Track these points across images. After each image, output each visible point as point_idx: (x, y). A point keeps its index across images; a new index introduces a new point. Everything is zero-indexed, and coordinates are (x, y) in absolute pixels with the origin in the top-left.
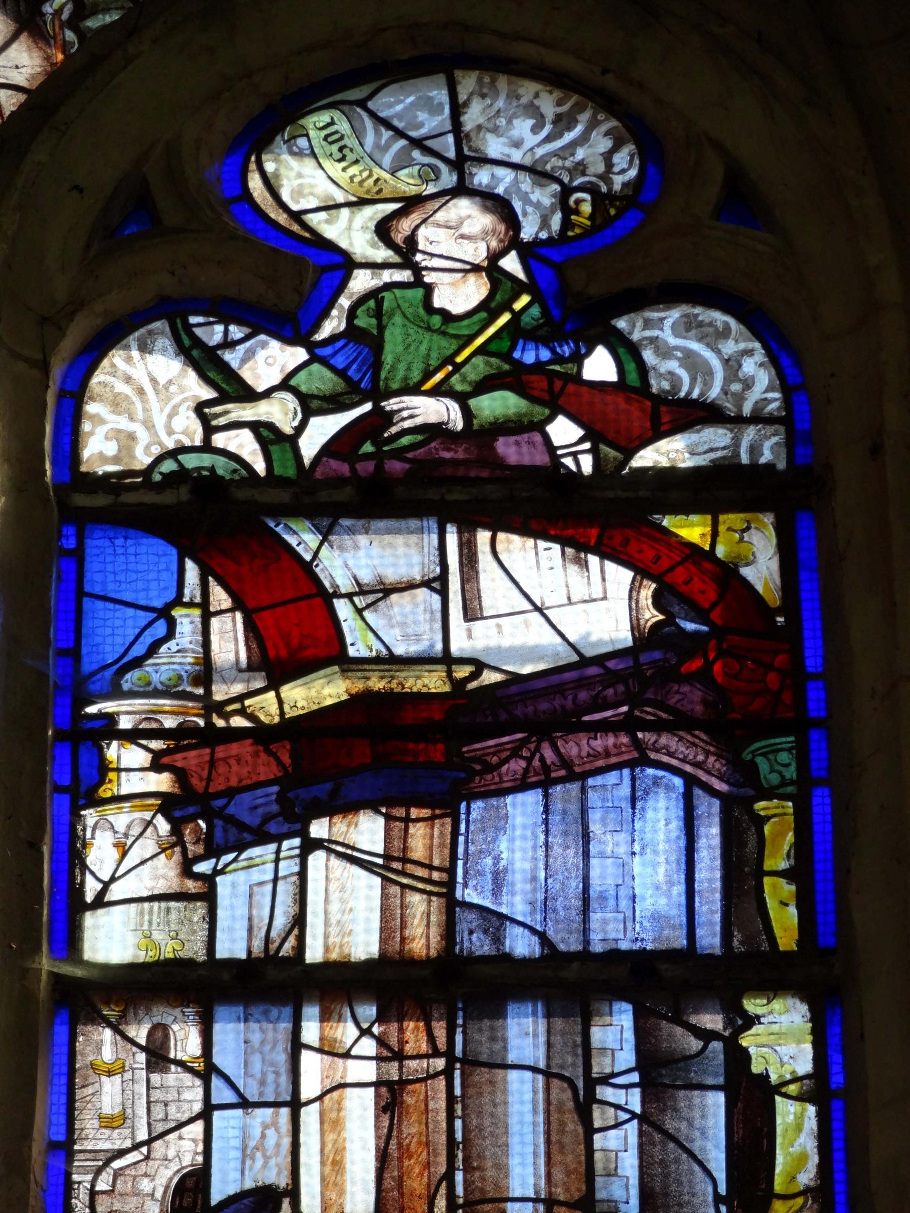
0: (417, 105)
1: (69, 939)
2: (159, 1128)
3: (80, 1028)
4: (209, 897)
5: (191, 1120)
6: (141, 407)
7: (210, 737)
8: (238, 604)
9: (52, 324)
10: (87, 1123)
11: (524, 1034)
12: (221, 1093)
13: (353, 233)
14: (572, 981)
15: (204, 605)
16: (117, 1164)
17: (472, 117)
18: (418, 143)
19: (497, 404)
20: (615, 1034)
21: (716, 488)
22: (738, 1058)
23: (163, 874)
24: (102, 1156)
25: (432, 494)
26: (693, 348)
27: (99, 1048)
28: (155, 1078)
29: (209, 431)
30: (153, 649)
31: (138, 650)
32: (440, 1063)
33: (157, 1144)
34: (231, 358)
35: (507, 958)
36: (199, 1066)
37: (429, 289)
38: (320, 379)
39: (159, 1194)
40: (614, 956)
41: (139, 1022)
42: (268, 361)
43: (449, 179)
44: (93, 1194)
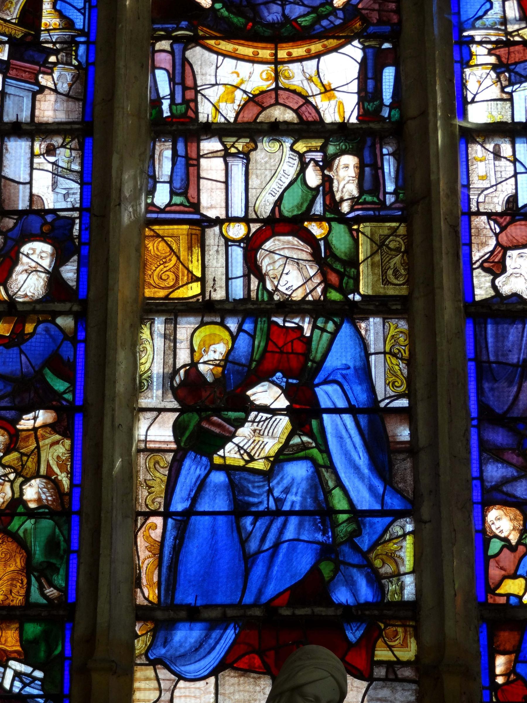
1: (463, 114)
2: (500, 180)
3: (469, 145)
4: (511, 100)
5: (510, 178)
7: (508, 44)
12: (520, 168)
16: (486, 192)
23: (495, 92)
24: (480, 190)
27: (476, 153)
28: (497, 163)
30: (486, 13)
31: (480, 13)
33: (499, 186)
36: (512, 159)
39: (501, 203)
41: (490, 143)
44: (478, 203)
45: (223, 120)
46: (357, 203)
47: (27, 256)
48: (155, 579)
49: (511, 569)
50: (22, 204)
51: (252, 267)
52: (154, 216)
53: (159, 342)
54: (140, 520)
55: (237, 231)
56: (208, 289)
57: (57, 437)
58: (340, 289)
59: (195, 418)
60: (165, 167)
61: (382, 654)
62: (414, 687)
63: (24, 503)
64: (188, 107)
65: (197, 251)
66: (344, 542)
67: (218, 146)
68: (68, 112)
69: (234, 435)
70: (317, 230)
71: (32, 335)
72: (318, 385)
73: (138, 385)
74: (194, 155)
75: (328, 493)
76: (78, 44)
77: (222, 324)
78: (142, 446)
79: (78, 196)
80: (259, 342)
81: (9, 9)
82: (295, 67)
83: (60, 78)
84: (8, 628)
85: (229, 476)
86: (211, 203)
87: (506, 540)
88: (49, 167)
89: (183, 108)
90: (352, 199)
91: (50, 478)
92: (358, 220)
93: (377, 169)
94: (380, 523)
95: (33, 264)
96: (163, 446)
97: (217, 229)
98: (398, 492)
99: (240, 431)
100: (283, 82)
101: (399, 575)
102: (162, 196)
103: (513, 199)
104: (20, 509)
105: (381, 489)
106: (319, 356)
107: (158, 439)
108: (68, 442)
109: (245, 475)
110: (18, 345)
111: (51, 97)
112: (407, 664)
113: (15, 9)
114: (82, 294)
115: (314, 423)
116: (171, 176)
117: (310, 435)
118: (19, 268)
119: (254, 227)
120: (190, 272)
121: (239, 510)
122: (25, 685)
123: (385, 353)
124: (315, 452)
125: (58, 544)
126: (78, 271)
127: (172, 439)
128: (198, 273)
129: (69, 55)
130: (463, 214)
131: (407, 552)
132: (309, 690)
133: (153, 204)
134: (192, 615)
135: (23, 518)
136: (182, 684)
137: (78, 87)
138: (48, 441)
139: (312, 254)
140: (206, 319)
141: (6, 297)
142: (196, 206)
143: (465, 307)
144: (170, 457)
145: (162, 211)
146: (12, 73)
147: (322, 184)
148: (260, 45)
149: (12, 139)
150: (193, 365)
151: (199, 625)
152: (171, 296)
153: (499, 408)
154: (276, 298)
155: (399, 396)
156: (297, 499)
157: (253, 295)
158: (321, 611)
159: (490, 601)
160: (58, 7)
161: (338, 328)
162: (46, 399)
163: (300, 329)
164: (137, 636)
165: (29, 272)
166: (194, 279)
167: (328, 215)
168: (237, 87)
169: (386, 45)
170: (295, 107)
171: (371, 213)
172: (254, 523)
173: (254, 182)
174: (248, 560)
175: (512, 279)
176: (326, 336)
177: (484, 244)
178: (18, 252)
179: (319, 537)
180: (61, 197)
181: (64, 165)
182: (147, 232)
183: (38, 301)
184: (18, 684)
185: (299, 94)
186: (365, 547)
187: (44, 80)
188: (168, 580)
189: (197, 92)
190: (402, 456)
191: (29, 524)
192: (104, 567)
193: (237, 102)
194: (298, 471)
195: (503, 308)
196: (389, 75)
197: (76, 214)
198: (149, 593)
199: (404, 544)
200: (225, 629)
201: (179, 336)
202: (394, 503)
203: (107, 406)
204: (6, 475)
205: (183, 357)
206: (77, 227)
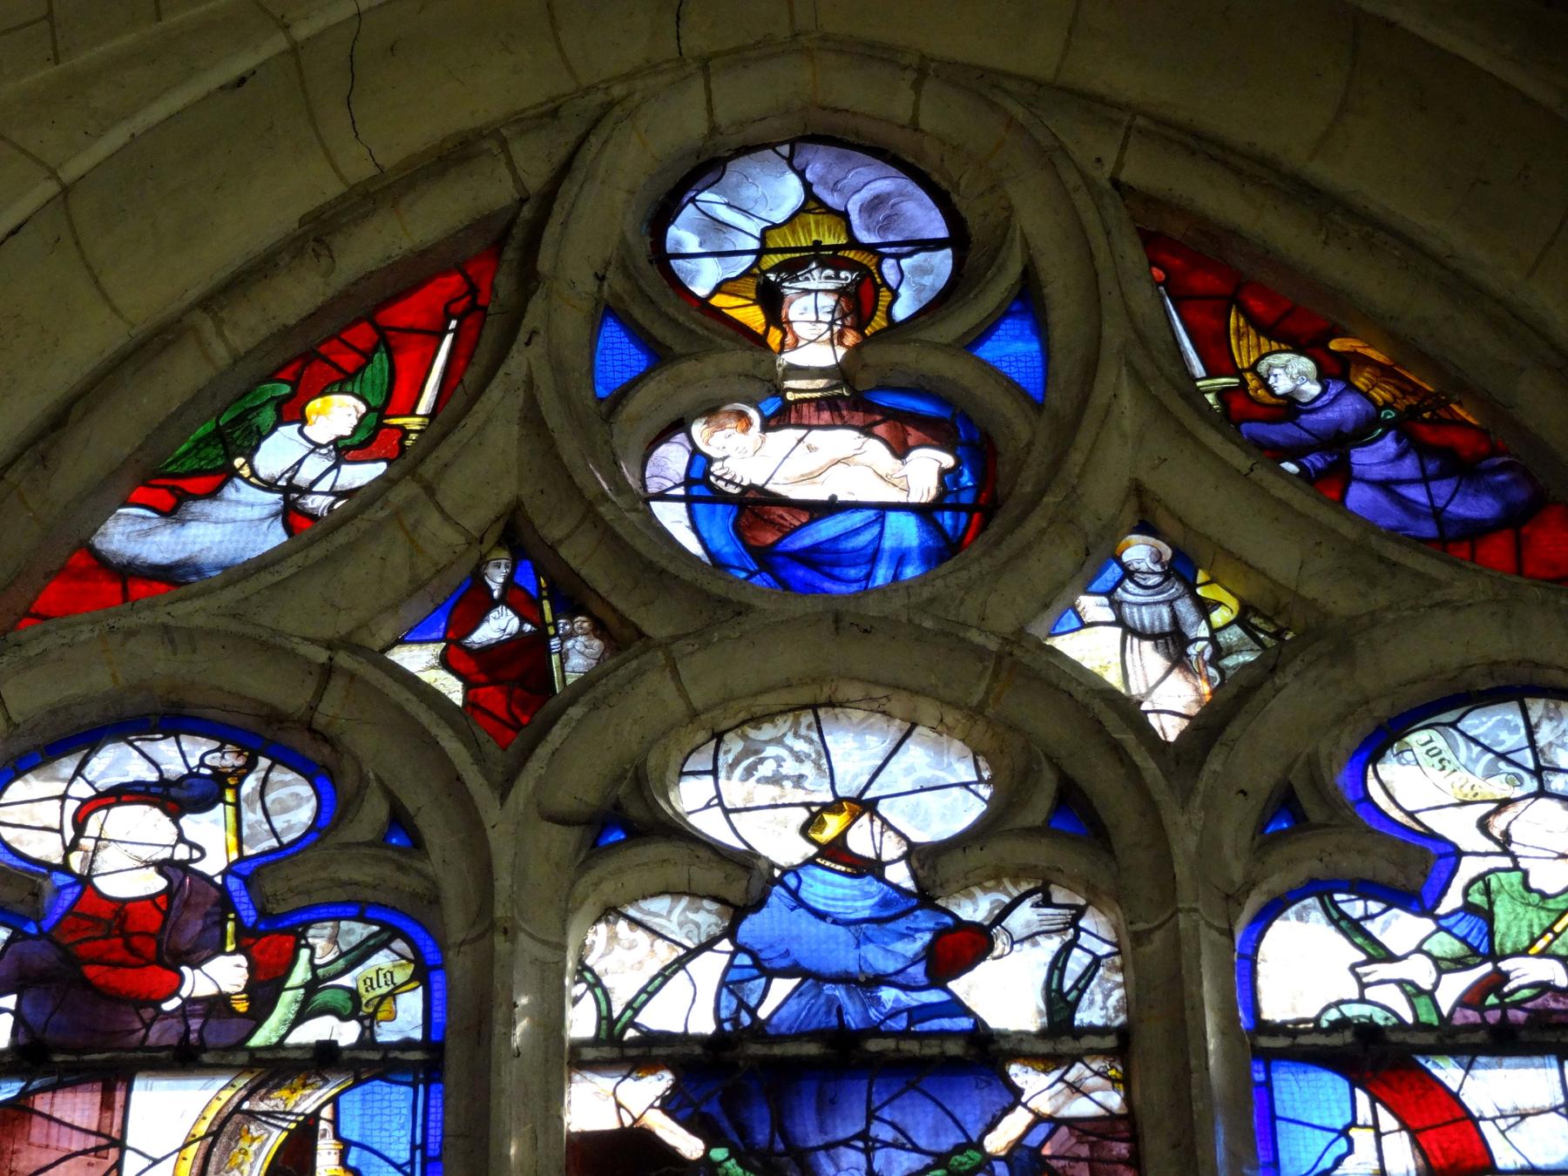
0: (1497, 725)
6: (1302, 968)
8: (1404, 1126)
9: (1233, 899)
13: (1458, 828)
15: (1376, 1126)
17: (1544, 735)
18: (1502, 756)
25: (1550, 1037)
29: (1363, 986)
30: (1338, 1161)
34: (1372, 927)
37: (1526, 874)
38: (1445, 945)
42: (1400, 929)
43: (1531, 785)
81: (239, 1166)
113: (252, 1166)
160: (352, 1162)
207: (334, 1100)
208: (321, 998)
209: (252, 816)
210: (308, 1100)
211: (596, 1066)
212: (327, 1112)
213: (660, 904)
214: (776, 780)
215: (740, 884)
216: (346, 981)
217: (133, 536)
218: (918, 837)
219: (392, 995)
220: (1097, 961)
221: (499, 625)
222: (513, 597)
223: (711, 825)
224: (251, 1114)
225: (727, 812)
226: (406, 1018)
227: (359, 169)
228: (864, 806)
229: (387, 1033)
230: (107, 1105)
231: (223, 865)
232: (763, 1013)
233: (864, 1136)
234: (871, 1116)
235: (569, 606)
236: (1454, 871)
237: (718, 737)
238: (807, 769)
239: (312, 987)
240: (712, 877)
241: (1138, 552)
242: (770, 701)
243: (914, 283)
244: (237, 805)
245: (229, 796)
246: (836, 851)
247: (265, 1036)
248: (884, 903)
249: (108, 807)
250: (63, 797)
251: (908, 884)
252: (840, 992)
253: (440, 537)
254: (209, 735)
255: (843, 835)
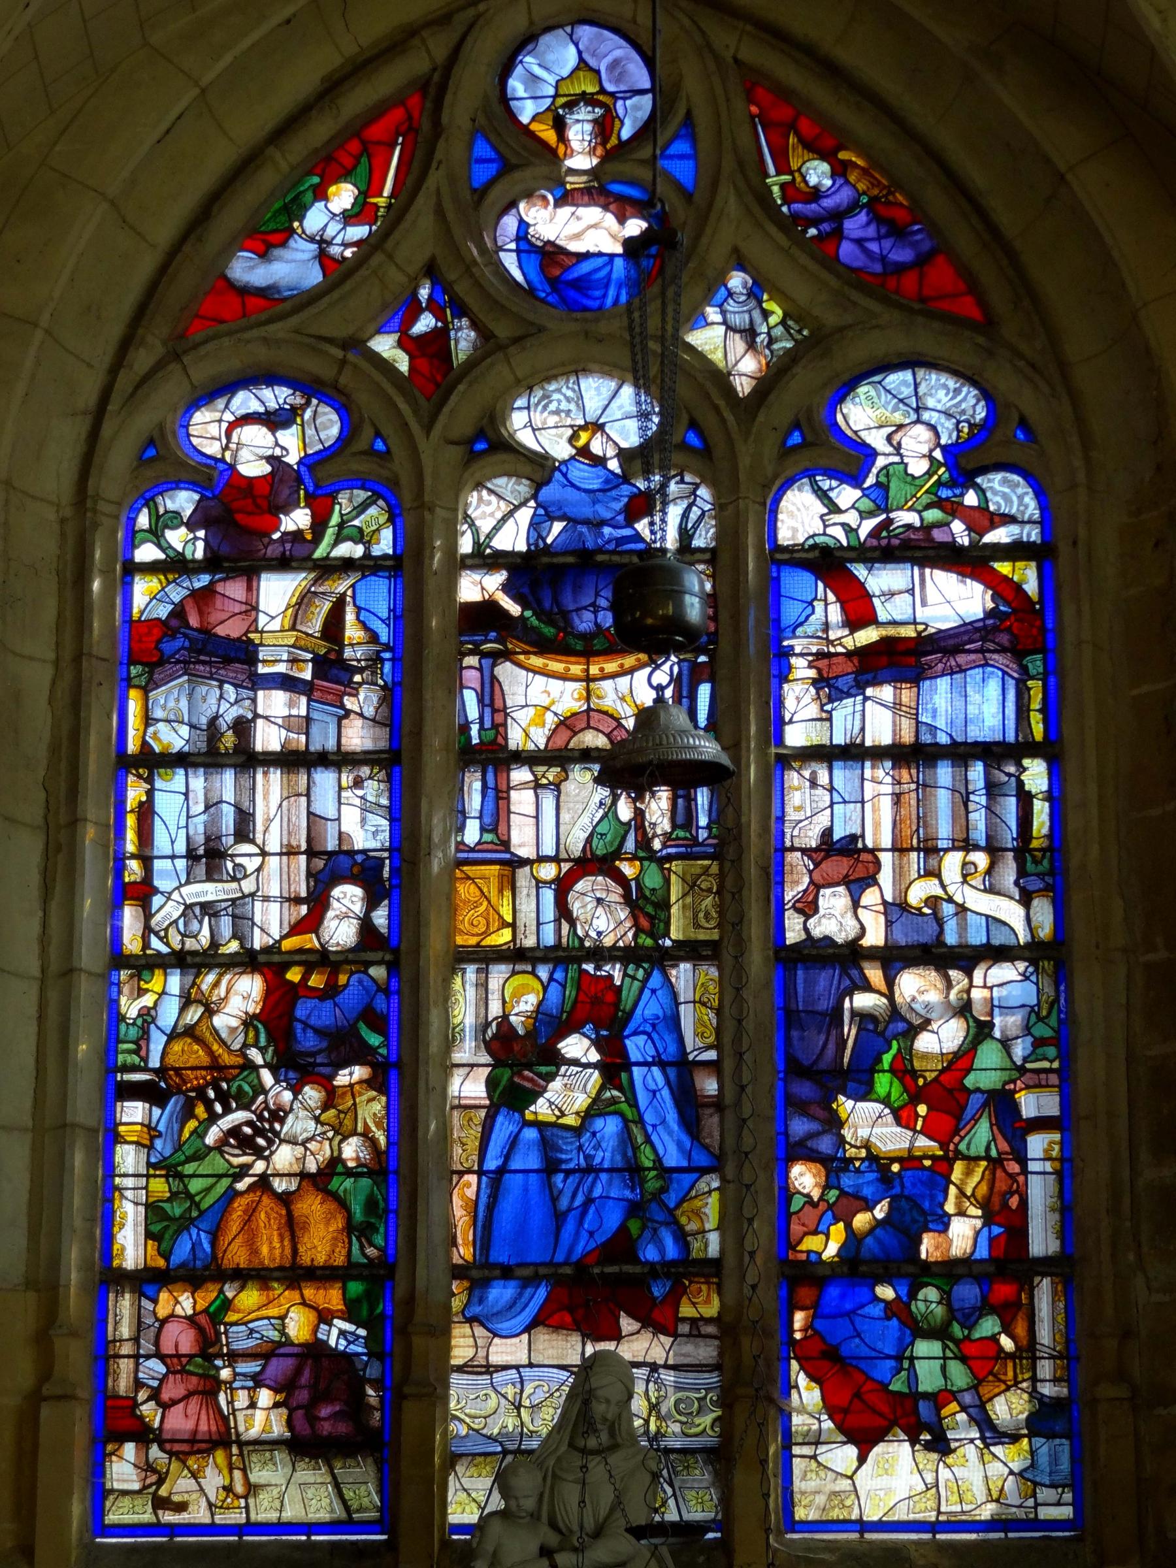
1: (779, 739)
4: (830, 719)
6: (800, 517)
7: (829, 655)
8: (839, 600)
9: (766, 486)
10: (789, 809)
11: (944, 773)
12: (837, 798)
13: (876, 440)
14: (962, 753)
15: (825, 600)
17: (922, 390)
18: (901, 401)
19: (933, 515)
20: (977, 773)
21: (1016, 551)
22: (1020, 784)
23: (813, 711)
25: (909, 554)
26: (1006, 492)
29: (825, 526)
31: (802, 619)
32: (913, 786)
34: (832, 494)
35: (937, 744)
37: (906, 465)
38: (866, 504)
40: (976, 743)
42: (846, 495)
43: (914, 417)
45: (533, 747)
46: (669, 839)
47: (338, 900)
48: (471, 1238)
49: (812, 1227)
50: (331, 845)
51: (563, 911)
52: (465, 855)
53: (471, 992)
54: (455, 1178)
55: (548, 871)
56: (520, 936)
57: (374, 1093)
58: (651, 934)
59: (507, 1073)
60: (474, 801)
61: (686, 1310)
62: (717, 1342)
63: (343, 1162)
64: (498, 732)
65: (508, 894)
66: (652, 1199)
67: (530, 777)
68: (375, 740)
69: (545, 1090)
70: (628, 870)
71: (346, 986)
72: (628, 1037)
73: (449, 1042)
74: (504, 788)
75: (636, 1149)
76: (382, 660)
77: (533, 973)
78: (456, 1102)
79: (387, 834)
80: (570, 992)
82: (607, 685)
83: (365, 700)
84: (332, 1287)
85: (540, 1132)
86: (522, 841)
87: (808, 1196)
88: (357, 802)
89: (492, 733)
90: (665, 834)
91: (366, 1135)
92: (670, 858)
93: (690, 801)
94: (688, 1178)
95: (344, 910)
96: (477, 1102)
97: (527, 869)
98: (706, 1148)
99: (551, 1086)
100: (595, 702)
101: (704, 1232)
102: (472, 833)
103: (828, 833)
104: (340, 1169)
105: (688, 1144)
106: (628, 1007)
107: (473, 1095)
108: (384, 1099)
109: (555, 1130)
110: (332, 997)
111: (358, 722)
112: (709, 1321)
114: (394, 942)
115: (624, 1075)
116: (481, 811)
117: (620, 1088)
118: (330, 914)
119: (565, 867)
120: (501, 917)
121: (551, 1166)
122: (349, 1343)
123: (694, 1002)
124: (624, 1107)
125: (376, 1203)
126: (390, 916)
127: (484, 1095)
128: (509, 919)
129: (374, 673)
130: (776, 850)
131: (712, 1207)
132: (600, 1393)
133: (462, 843)
134: (507, 1272)
135: (341, 1178)
136: (496, 1340)
137: (385, 710)
138: (365, 1098)
139: (623, 896)
140: (518, 967)
141: (317, 945)
142: (506, 844)
143: (776, 953)
144: (483, 1113)
145: (472, 850)
146: (317, 695)
147: (634, 819)
148: (573, 659)
149: (319, 769)
150: (505, 1017)
151: (513, 1283)
152: (483, 943)
153: (806, 1060)
154: (587, 944)
155: (708, 1048)
156: (608, 1155)
157: (564, 940)
158: (629, 1269)
159: (791, 1257)
161: (648, 975)
162: (360, 1054)
163: (610, 977)
164: (454, 1295)
165: (342, 917)
166: (504, 924)
167: (641, 854)
168: (547, 709)
169: (702, 659)
170: (607, 731)
171: (683, 850)
172: (565, 1181)
173: (565, 817)
174: (559, 1218)
175: (823, 920)
176: (637, 984)
177: (797, 883)
178: (329, 896)
179: (628, 1194)
180: (370, 835)
181: (372, 799)
182: (458, 874)
183: (351, 950)
184: (343, 1342)
185: (612, 716)
186: (672, 1205)
187: (349, 703)
188: (482, 1238)
189: (507, 715)
190: (711, 1110)
191: (349, 1183)
192: (421, 1232)
193: (548, 726)
194: (609, 1127)
195: (814, 952)
196: (704, 692)
197: (386, 854)
198: (464, 1252)
199: (710, 1200)
200: (537, 1287)
201: (490, 986)
202: (701, 1159)
203: (421, 1069)
204: (324, 1133)
205: (495, 1009)
206: (387, 869)
207: (353, 586)
208: (345, 532)
209: (310, 432)
210: (342, 586)
211: (472, 568)
212: (349, 593)
213: (502, 481)
214: (557, 412)
215: (538, 469)
216: (356, 522)
217: (247, 270)
218: (624, 445)
219: (378, 530)
220: (703, 512)
221: (425, 323)
222: (434, 307)
223: (526, 438)
224: (315, 593)
225: (534, 430)
226: (385, 544)
227: (350, 49)
228: (597, 427)
229: (376, 551)
230: (249, 588)
231: (297, 459)
232: (549, 540)
233: (593, 604)
234: (597, 595)
235: (461, 311)
236: (873, 463)
237: (531, 388)
238: (572, 407)
239: (341, 526)
240: (528, 469)
241: (737, 281)
242: (555, 372)
243: (633, 115)
244: (302, 425)
245: (299, 420)
246: (584, 451)
247: (319, 553)
248: (607, 481)
249: (241, 426)
250: (220, 421)
251: (618, 471)
252: (584, 529)
253: (396, 278)
254: (289, 387)
255: (587, 444)
